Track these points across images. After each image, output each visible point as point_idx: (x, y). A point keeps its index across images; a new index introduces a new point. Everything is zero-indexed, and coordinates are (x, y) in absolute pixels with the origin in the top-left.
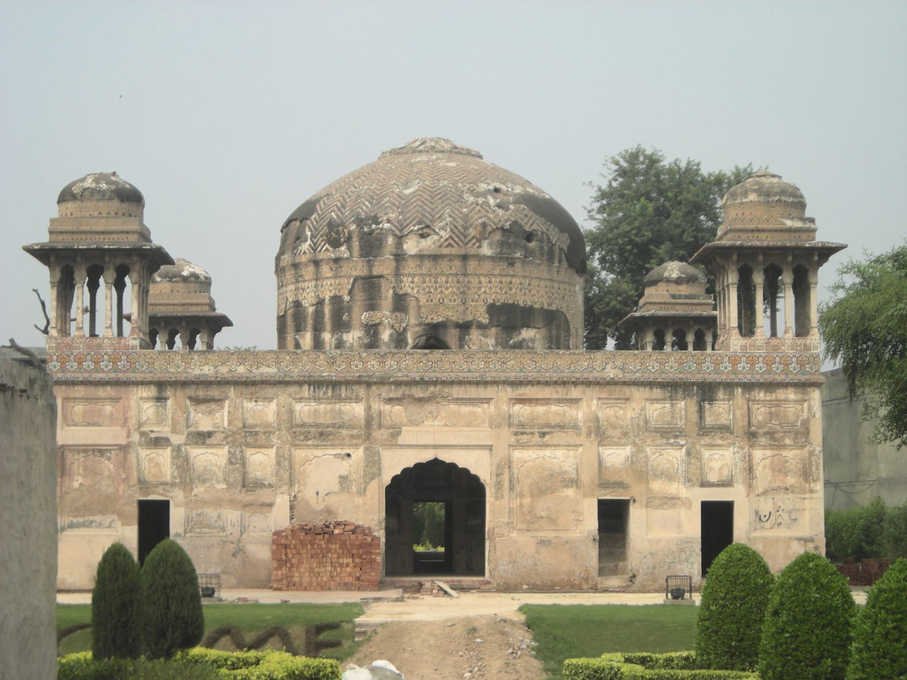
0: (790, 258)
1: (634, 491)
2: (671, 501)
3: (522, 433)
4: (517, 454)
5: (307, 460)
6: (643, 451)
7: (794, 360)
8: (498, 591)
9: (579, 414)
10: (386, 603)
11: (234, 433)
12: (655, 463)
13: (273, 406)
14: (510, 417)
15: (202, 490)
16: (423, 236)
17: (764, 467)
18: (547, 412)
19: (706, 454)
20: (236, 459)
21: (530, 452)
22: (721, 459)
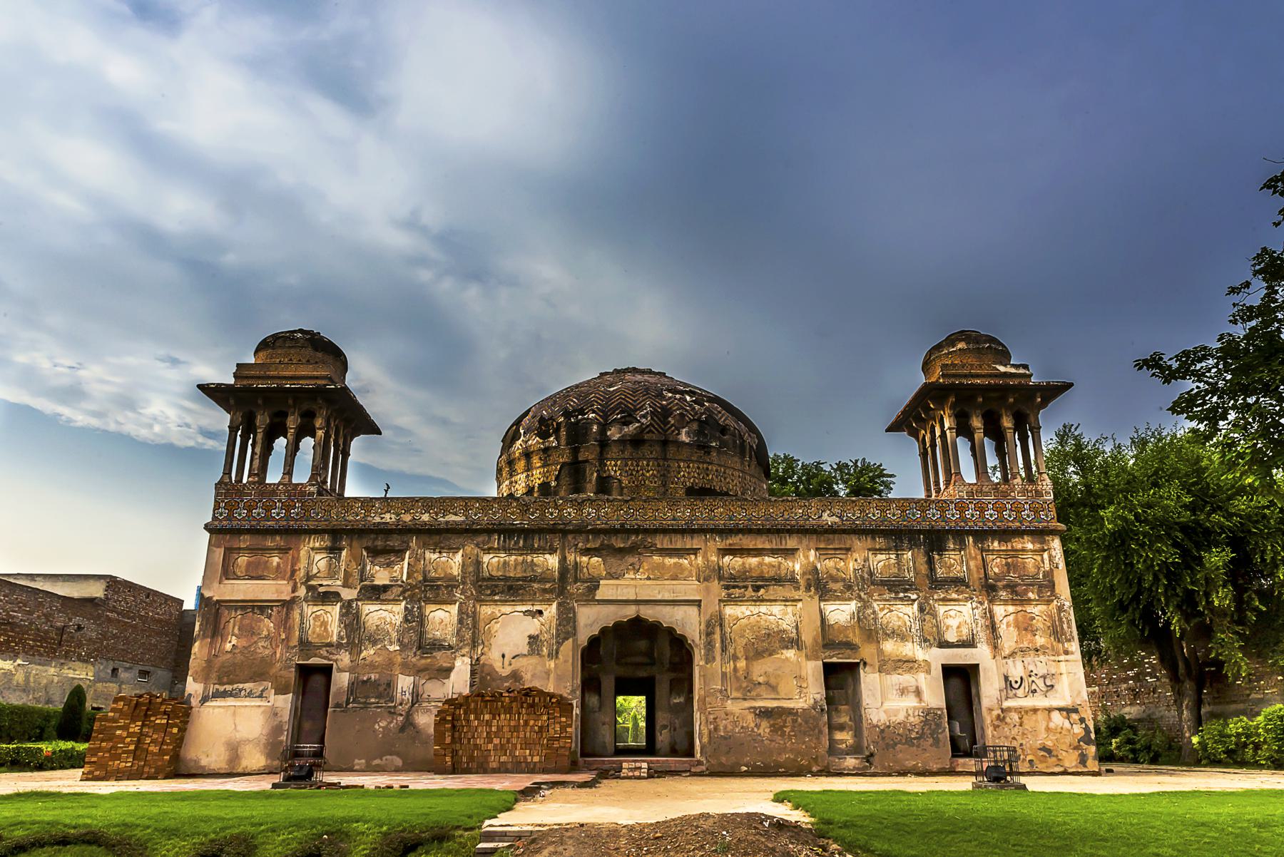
0: (1011, 400)
1: (867, 652)
2: (908, 664)
3: (734, 587)
4: (730, 611)
5: (493, 618)
6: (871, 606)
7: (1027, 506)
8: (713, 774)
9: (796, 566)
10: (568, 790)
11: (413, 587)
12: (885, 621)
13: (458, 557)
14: (720, 568)
15: (372, 652)
16: (627, 424)
17: (1008, 625)
18: (760, 564)
19: (941, 610)
20: (413, 616)
21: (744, 608)
22: (959, 616)
